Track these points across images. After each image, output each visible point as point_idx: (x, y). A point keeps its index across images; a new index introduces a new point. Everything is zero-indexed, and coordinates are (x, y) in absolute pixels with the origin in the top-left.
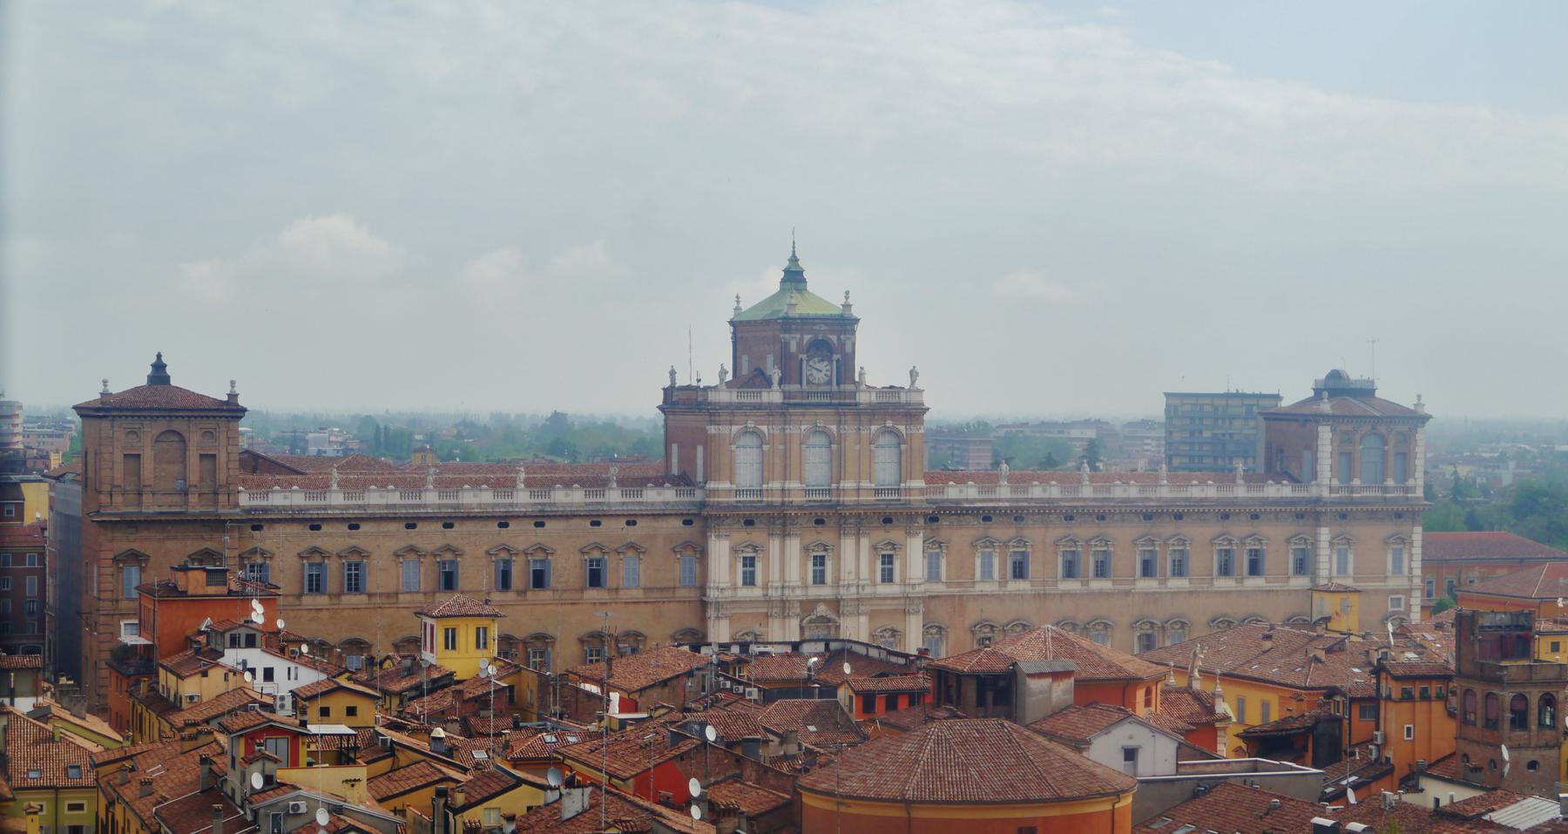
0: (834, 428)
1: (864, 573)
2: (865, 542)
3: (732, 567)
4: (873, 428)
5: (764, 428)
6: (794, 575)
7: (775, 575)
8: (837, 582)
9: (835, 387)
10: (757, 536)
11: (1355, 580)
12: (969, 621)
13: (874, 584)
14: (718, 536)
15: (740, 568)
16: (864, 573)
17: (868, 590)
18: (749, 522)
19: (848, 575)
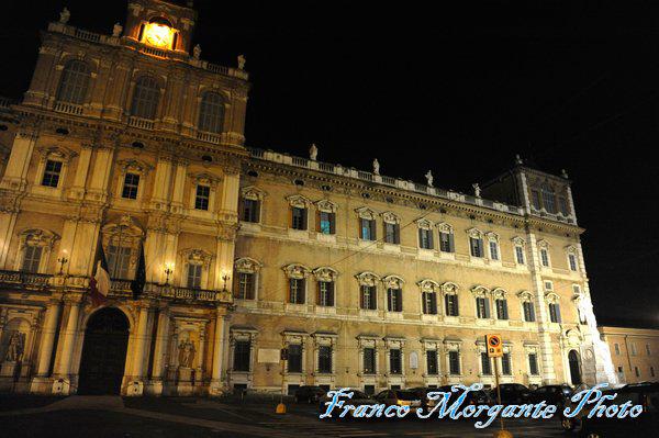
0: (165, 77)
1: (178, 196)
2: (181, 172)
3: (32, 165)
4: (201, 86)
5: (98, 62)
6: (100, 181)
7: (80, 180)
8: (147, 199)
9: (170, 48)
10: (68, 143)
11: (554, 271)
12: (281, 263)
13: (186, 207)
14: (23, 135)
15: (41, 168)
16: (178, 196)
17: (180, 212)
18: (63, 131)
19: (160, 192)
